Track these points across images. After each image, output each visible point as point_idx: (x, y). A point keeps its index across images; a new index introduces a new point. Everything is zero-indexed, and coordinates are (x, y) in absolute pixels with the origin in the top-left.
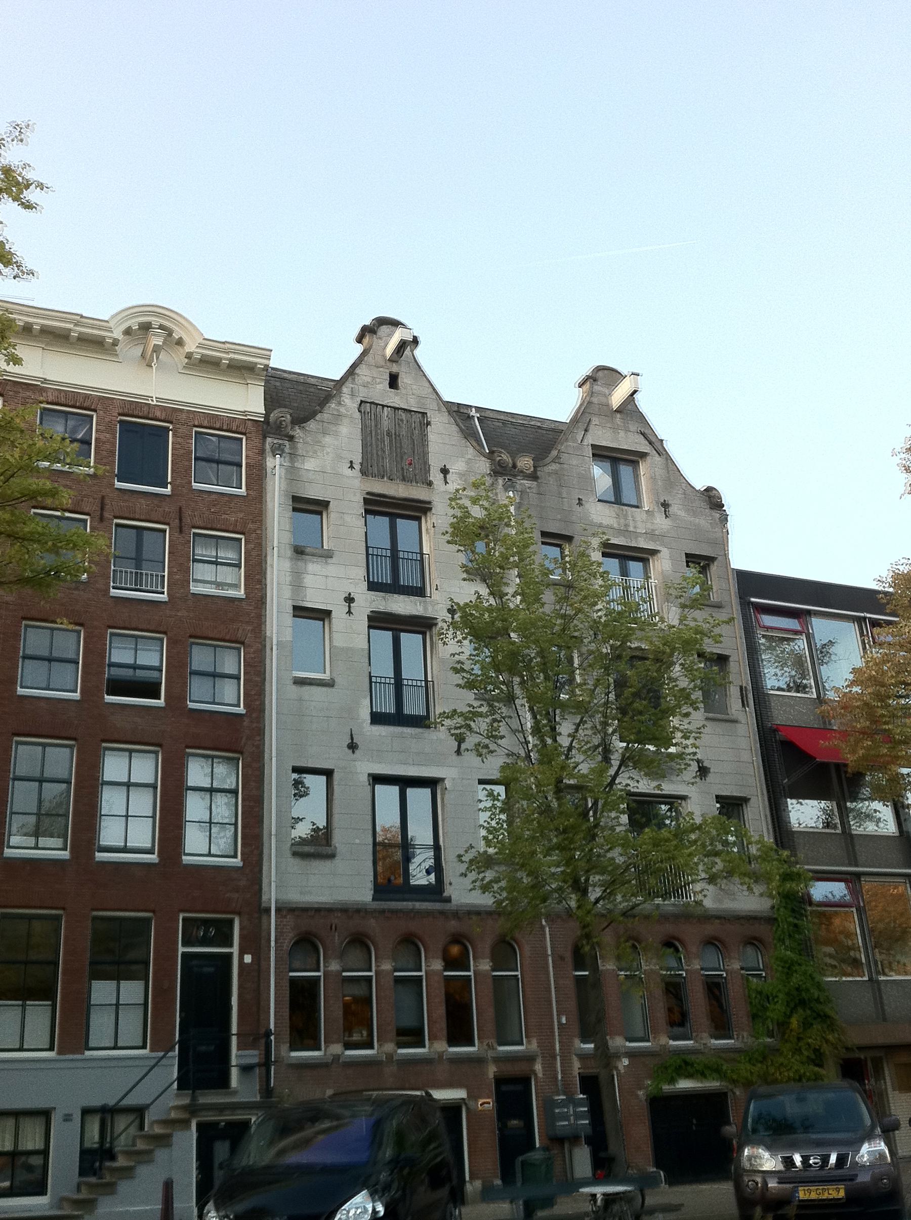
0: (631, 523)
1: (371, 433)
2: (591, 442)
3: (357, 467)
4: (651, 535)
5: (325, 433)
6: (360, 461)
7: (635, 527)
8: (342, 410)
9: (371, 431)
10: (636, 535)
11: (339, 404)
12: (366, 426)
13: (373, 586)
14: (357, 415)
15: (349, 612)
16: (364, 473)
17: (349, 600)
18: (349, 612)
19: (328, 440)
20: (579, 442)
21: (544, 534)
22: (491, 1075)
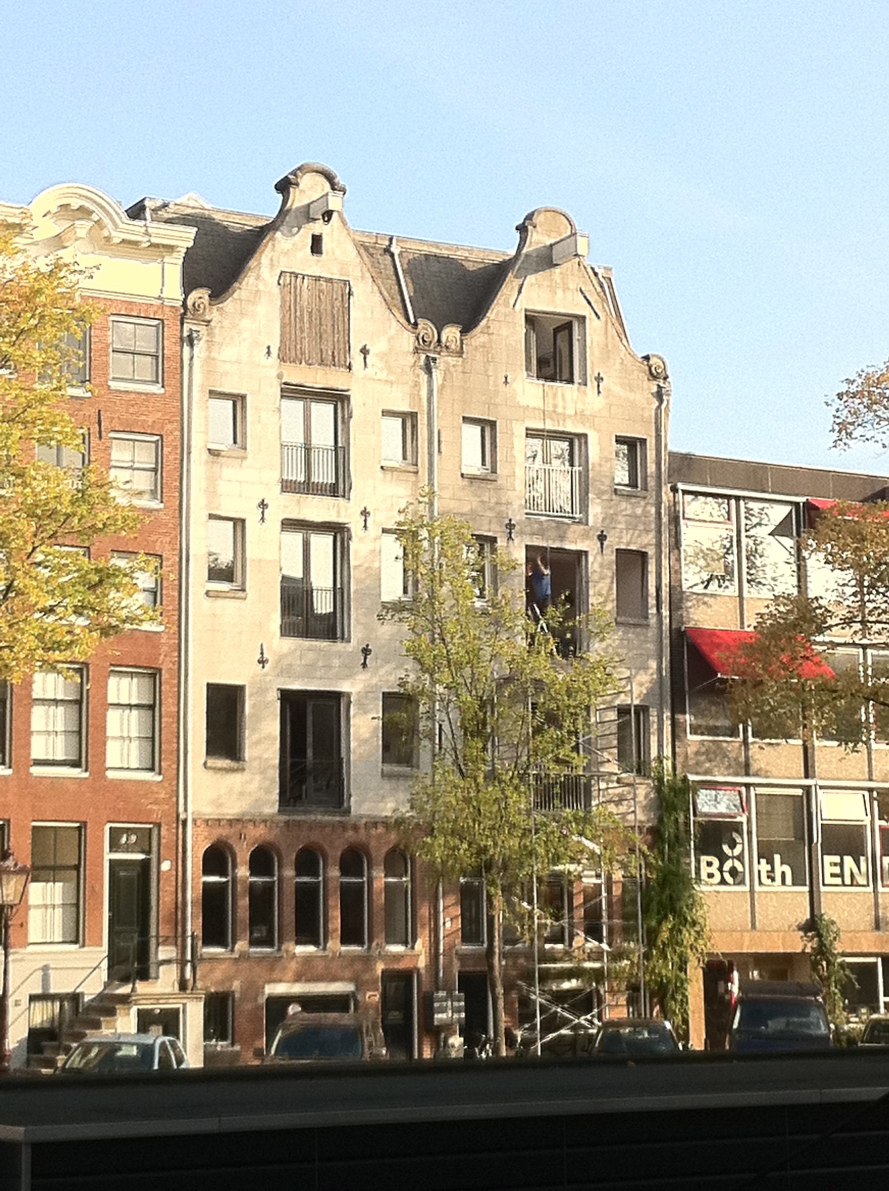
0: (560, 403)
1: (290, 310)
2: (525, 306)
3: (275, 351)
4: (580, 416)
5: (242, 314)
6: (278, 345)
7: (564, 408)
8: (261, 287)
9: (290, 307)
10: (565, 417)
11: (258, 277)
12: (285, 301)
13: (287, 487)
14: (276, 290)
15: (263, 519)
16: (282, 359)
17: (263, 505)
18: (263, 519)
19: (245, 323)
20: (511, 306)
21: (464, 418)
22: (379, 972)
